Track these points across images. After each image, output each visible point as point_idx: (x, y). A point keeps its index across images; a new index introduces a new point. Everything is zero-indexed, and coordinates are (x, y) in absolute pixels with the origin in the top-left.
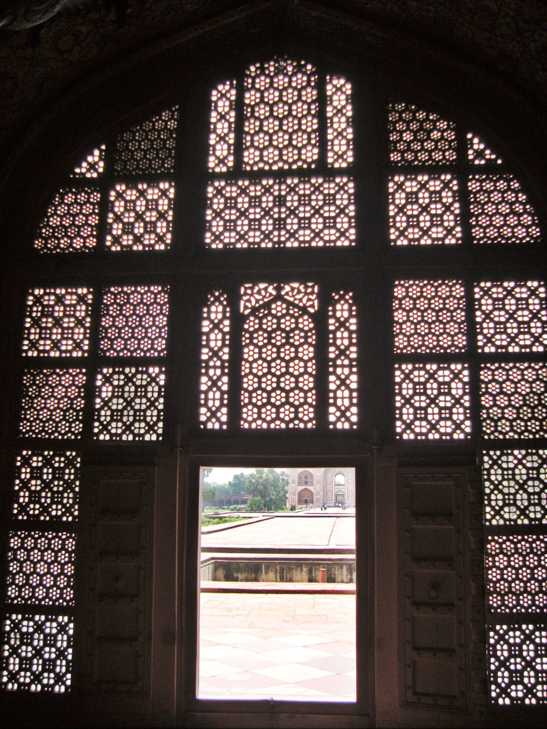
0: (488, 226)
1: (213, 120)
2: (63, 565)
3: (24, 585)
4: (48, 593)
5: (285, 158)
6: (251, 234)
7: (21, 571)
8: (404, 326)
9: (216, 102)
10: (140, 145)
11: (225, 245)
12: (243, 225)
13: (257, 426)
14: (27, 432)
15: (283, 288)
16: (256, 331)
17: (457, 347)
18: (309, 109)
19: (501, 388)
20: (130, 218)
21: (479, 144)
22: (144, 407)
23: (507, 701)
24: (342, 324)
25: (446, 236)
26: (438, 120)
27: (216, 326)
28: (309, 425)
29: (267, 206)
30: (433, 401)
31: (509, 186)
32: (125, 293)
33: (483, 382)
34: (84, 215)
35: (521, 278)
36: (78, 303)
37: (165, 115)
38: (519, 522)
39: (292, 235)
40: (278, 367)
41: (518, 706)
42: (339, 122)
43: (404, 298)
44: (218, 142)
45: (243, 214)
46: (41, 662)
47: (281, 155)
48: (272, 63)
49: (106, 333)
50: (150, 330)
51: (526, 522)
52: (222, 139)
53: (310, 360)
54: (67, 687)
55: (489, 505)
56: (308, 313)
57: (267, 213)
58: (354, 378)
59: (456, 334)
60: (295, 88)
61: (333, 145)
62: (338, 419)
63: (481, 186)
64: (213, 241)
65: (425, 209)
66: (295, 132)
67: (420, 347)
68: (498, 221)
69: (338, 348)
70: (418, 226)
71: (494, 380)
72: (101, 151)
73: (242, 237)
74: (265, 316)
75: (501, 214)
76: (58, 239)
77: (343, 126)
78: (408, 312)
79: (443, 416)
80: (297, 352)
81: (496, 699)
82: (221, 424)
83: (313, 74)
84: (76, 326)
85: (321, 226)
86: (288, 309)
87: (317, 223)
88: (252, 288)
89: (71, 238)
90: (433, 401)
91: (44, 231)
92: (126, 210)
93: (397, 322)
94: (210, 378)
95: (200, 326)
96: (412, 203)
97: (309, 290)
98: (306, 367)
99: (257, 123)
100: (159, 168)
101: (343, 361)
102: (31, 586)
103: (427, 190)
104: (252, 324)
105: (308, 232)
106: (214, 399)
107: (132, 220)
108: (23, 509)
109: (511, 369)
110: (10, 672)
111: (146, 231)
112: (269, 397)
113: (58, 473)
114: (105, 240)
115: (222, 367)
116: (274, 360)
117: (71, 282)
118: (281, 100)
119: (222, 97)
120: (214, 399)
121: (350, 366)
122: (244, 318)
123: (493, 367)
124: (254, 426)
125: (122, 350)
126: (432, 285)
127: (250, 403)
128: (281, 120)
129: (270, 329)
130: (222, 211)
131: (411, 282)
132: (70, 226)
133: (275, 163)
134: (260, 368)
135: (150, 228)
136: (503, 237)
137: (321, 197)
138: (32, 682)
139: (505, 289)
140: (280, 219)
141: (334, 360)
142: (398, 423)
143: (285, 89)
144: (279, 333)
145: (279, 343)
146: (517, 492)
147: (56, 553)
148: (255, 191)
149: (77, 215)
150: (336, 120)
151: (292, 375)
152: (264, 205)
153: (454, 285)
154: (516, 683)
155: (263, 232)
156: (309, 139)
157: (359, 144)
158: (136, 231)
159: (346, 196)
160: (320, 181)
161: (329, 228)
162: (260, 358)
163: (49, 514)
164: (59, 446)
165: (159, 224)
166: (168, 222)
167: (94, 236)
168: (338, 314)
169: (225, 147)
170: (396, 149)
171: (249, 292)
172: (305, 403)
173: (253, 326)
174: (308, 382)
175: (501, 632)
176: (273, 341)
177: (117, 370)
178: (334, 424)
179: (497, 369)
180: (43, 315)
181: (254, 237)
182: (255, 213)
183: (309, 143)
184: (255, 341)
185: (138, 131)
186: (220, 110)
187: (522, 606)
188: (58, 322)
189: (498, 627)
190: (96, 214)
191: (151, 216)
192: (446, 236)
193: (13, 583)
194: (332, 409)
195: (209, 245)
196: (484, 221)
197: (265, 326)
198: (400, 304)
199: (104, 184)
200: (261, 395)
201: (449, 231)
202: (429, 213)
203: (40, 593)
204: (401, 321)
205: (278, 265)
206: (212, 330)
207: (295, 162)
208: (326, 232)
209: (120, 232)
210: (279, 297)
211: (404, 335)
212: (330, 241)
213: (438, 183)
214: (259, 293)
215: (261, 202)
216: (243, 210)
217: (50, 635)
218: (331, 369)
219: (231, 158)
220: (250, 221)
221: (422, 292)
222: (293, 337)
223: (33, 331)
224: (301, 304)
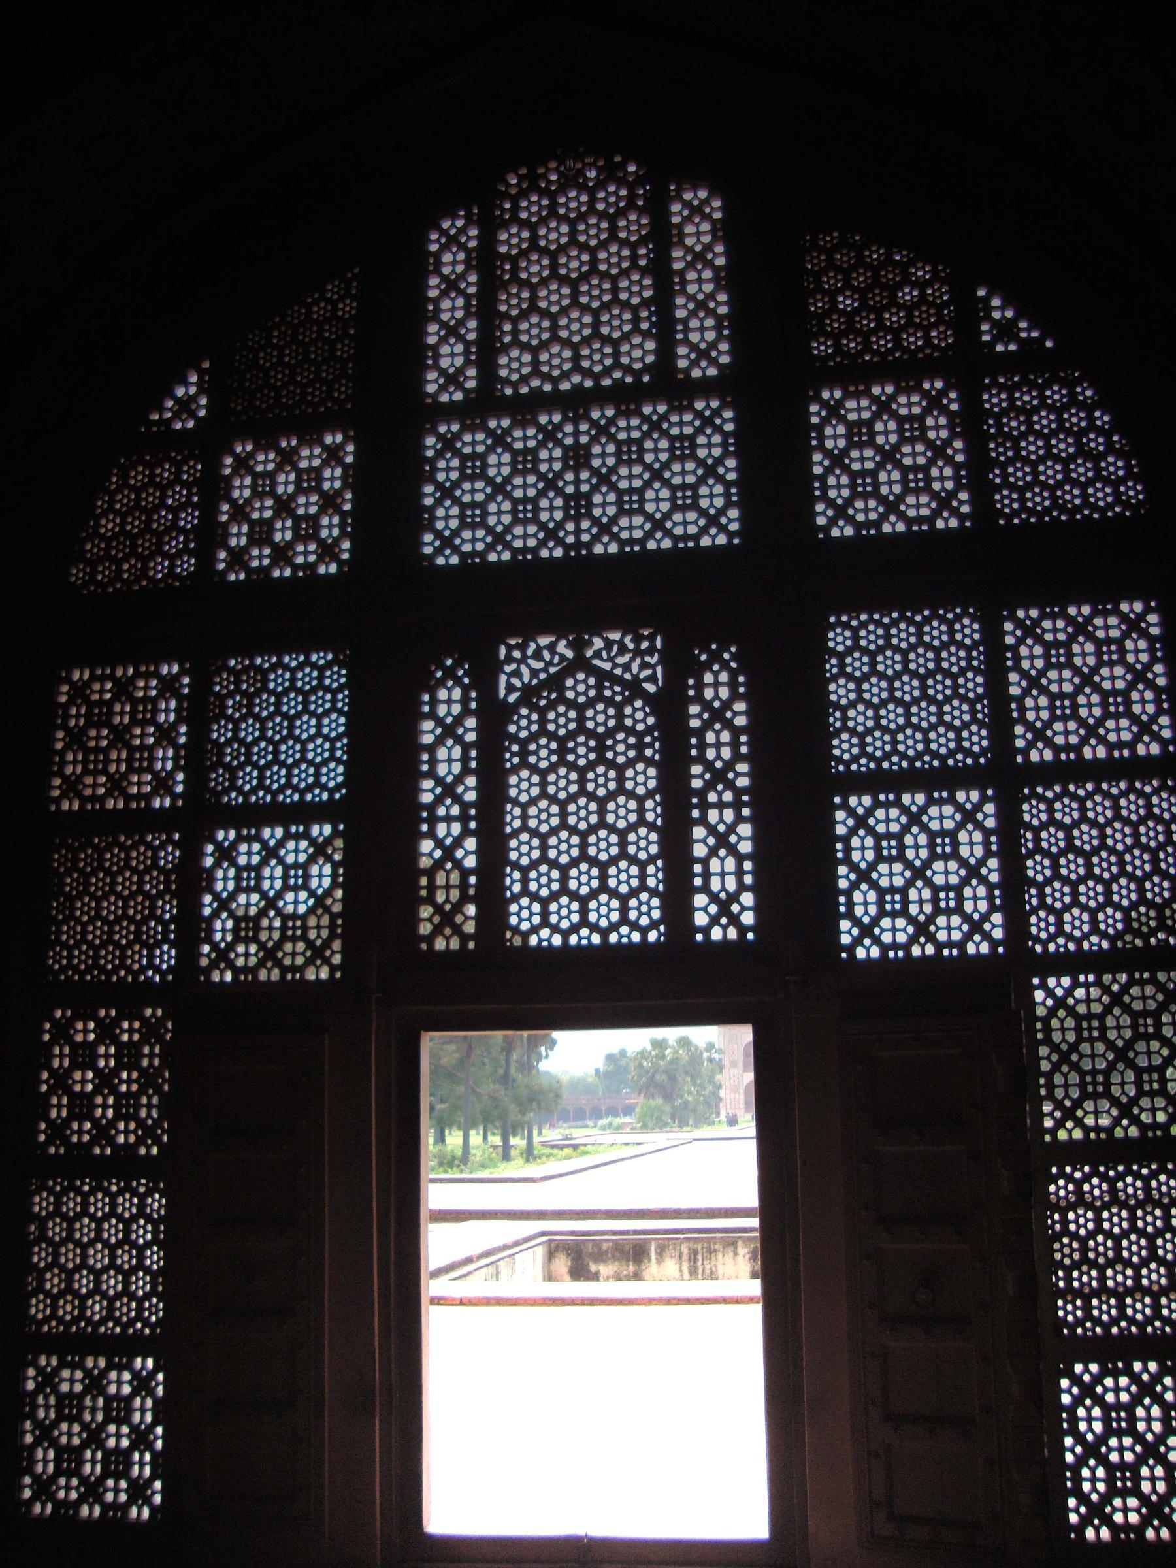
0: (1029, 486)
2: (141, 1250)
3: (62, 1294)
4: (111, 1309)
5: (586, 364)
6: (518, 530)
7: (55, 1263)
8: (851, 713)
9: (437, 255)
10: (281, 356)
11: (464, 556)
12: (500, 513)
13: (541, 941)
14: (63, 969)
15: (590, 643)
16: (533, 737)
17: (968, 753)
18: (634, 258)
19: (1069, 838)
20: (264, 510)
21: (1002, 308)
23: (1105, 1533)
24: (717, 715)
25: (936, 513)
26: (911, 262)
27: (449, 731)
28: (652, 936)
29: (551, 469)
30: (919, 873)
31: (1072, 395)
32: (259, 669)
33: (1029, 826)
34: (170, 509)
35: (1104, 597)
36: (161, 695)
37: (332, 289)
38: (1119, 1133)
39: (605, 529)
40: (583, 814)
41: (1128, 1542)
42: (700, 281)
43: (849, 651)
44: (443, 340)
45: (500, 489)
46: (99, 1455)
47: (576, 358)
48: (553, 165)
50: (311, 746)
51: (1134, 1132)
52: (452, 331)
53: (650, 794)
54: (154, 1510)
55: (1051, 1096)
56: (644, 695)
57: (550, 483)
58: (745, 829)
59: (966, 725)
60: (602, 215)
61: (687, 330)
62: (714, 921)
63: (1011, 400)
64: (439, 551)
65: (889, 456)
66: (606, 306)
68: (1051, 472)
70: (876, 494)
72: (201, 373)
73: (499, 538)
74: (552, 705)
75: (1057, 459)
76: (119, 563)
77: (708, 288)
78: (859, 682)
79: (952, 904)
80: (621, 779)
81: (1080, 1529)
82: (465, 938)
83: (640, 180)
84: (158, 743)
85: (665, 507)
86: (599, 687)
87: (657, 500)
88: (523, 647)
89: (145, 560)
90: (919, 873)
92: (257, 494)
93: (837, 706)
94: (439, 843)
95: (416, 733)
96: (861, 446)
97: (645, 645)
98: (641, 811)
99: (525, 295)
101: (720, 794)
102: (76, 1294)
103: (894, 415)
104: (524, 723)
105: (638, 520)
106: (448, 887)
107: (268, 514)
108: (58, 1131)
109: (1089, 795)
110: (36, 1478)
111: (297, 537)
112: (564, 879)
113: (128, 1056)
114: (215, 560)
115: (464, 818)
116: (572, 798)
117: (147, 654)
118: (573, 241)
120: (448, 887)
121: (737, 805)
122: (507, 712)
123: (1049, 794)
124: (533, 940)
125: (254, 790)
126: (910, 622)
127: (525, 891)
128: (574, 284)
129: (562, 732)
130: (456, 484)
131: (864, 617)
132: (141, 534)
133: (565, 375)
135: (307, 528)
136: (1062, 509)
137: (664, 444)
138: (82, 1499)
139: (1070, 620)
140: (578, 495)
141: (702, 793)
142: (845, 925)
143: (582, 217)
144: (581, 739)
145: (582, 762)
146: (1112, 1066)
147: (127, 1223)
148: (525, 438)
149: (156, 509)
150: (691, 275)
151: (612, 829)
152: (543, 468)
153: (958, 618)
154: (1124, 1494)
155: (542, 526)
156: (636, 320)
158: (278, 537)
159: (717, 439)
160: (662, 409)
161: (684, 508)
162: (544, 794)
163: (111, 1142)
164: (131, 997)
165: (325, 521)
166: (343, 515)
167: (191, 553)
168: (709, 694)
169: (459, 348)
170: (822, 332)
171: (517, 654)
172: (643, 887)
173: (527, 728)
174: (646, 843)
175: (1087, 1378)
176: (571, 758)
178: (706, 930)
179: (1058, 797)
180: (90, 724)
181: (525, 536)
182: (525, 486)
183: (636, 329)
184: (532, 759)
186: (446, 270)
187: (1132, 1321)
188: (120, 736)
189: (1078, 1368)
190: (195, 506)
191: (307, 504)
192: (936, 513)
193: (40, 1289)
194: (700, 900)
195: (431, 558)
197: (551, 727)
198: (842, 666)
199: (209, 442)
200: (548, 874)
201: (944, 502)
202: (898, 465)
203: (96, 1308)
204: (844, 702)
205: (574, 593)
206: (440, 741)
207: (607, 371)
208: (678, 517)
209: (243, 541)
210: (580, 663)
211: (853, 732)
212: (686, 537)
213: (915, 399)
214: (537, 655)
215: (536, 461)
216: (499, 480)
217: (118, 1397)
218: (696, 814)
219: (472, 372)
220: (515, 502)
223: (70, 757)
224: (628, 676)
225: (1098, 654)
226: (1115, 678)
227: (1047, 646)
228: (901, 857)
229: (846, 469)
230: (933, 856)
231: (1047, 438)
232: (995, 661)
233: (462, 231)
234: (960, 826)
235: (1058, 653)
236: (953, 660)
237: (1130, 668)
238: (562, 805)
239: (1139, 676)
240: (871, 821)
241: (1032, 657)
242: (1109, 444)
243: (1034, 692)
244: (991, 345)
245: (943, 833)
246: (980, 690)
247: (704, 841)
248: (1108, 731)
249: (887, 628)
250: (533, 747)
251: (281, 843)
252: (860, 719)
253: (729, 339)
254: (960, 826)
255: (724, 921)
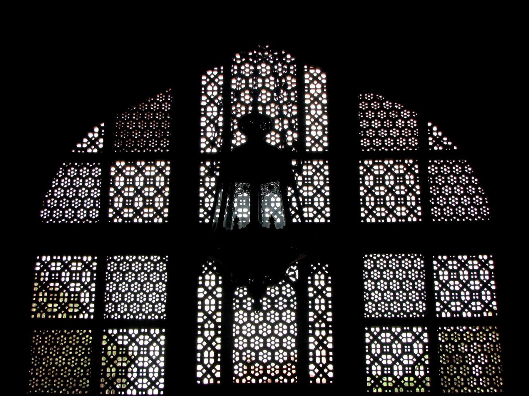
1: (203, 104)
10: (137, 125)
13: (247, 381)
17: (418, 312)
22: (146, 365)
24: (320, 292)
25: (408, 215)
26: (402, 110)
28: (292, 380)
30: (398, 359)
32: (128, 261)
43: (372, 269)
49: (111, 297)
53: (292, 323)
58: (330, 339)
59: (417, 301)
61: (310, 130)
67: (386, 312)
69: (316, 313)
71: (450, 341)
72: (101, 128)
78: (376, 282)
80: (280, 316)
82: (216, 379)
90: (398, 359)
91: (49, 201)
93: (367, 291)
94: (205, 339)
98: (289, 330)
100: (156, 148)
101: (320, 324)
103: (393, 173)
106: (209, 358)
115: (216, 329)
119: (211, 84)
120: (209, 358)
121: (327, 329)
126: (397, 258)
127: (241, 360)
134: (248, 330)
135: (148, 202)
139: (459, 262)
141: (313, 324)
151: (277, 336)
153: (415, 258)
157: (333, 131)
168: (316, 283)
174: (290, 343)
177: (121, 331)
184: (245, 306)
185: (135, 111)
190: (98, 188)
191: (150, 192)
194: (312, 367)
196: (441, 201)
199: (105, 159)
200: (250, 354)
201: (411, 210)
202: (394, 194)
206: (206, 297)
211: (373, 302)
218: (310, 332)
221: (388, 264)
222: (277, 303)
225: (469, 275)
226: (475, 285)
227: (450, 271)
228: (391, 353)
229: (373, 194)
230: (403, 353)
231: (452, 187)
232: (429, 277)
233: (216, 77)
234: (414, 341)
235: (454, 274)
236: (413, 274)
237: (481, 282)
238: (257, 326)
239: (485, 285)
240: (380, 338)
241: (443, 275)
242: (477, 190)
243: (444, 289)
244: (432, 147)
245: (407, 344)
246: (423, 287)
247: (313, 343)
248: (472, 306)
249: (387, 260)
250: (245, 301)
251: (137, 336)
252: (376, 297)
253: (328, 135)
254: (414, 341)
255: (321, 375)
